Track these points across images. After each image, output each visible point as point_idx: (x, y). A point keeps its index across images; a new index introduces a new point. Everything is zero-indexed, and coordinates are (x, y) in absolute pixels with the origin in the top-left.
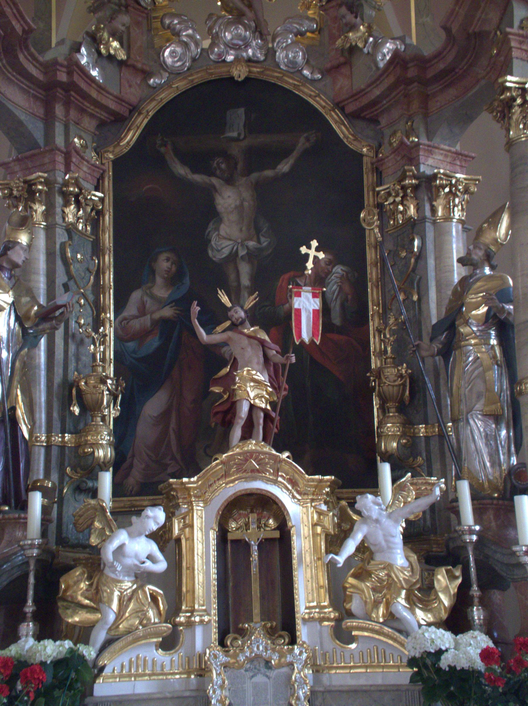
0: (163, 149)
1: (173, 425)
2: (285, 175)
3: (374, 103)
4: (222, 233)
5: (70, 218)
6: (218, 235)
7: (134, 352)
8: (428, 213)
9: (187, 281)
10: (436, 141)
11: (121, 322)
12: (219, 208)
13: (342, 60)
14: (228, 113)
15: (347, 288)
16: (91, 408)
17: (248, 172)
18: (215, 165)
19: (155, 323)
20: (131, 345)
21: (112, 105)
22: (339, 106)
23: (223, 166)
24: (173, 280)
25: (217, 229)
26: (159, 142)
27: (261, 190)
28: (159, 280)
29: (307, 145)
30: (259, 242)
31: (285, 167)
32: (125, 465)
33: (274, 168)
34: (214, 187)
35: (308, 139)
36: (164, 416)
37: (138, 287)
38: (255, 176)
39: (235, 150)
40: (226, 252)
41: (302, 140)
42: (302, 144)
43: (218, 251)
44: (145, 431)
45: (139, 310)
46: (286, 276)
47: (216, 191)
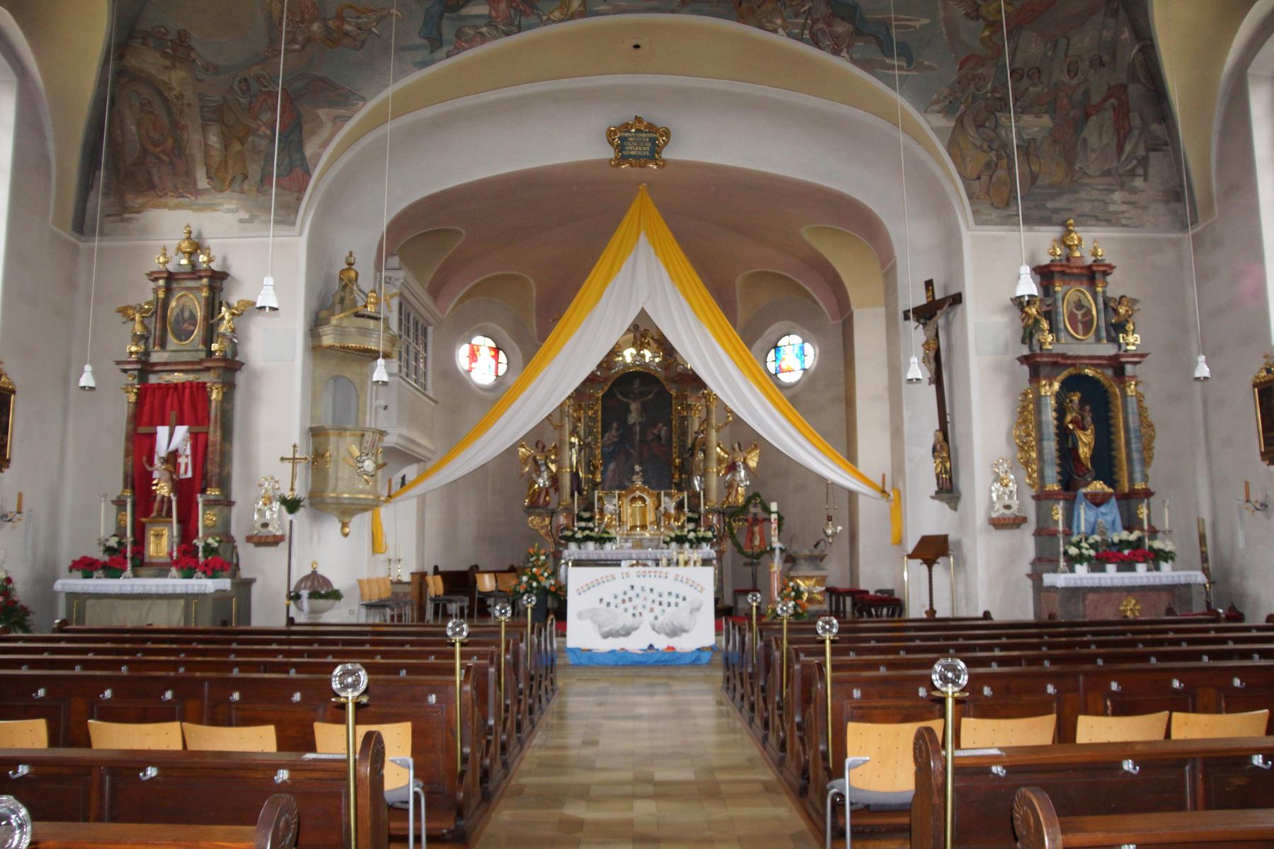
16: (596, 468)
36: (614, 471)
42: (656, 389)
44: (609, 473)
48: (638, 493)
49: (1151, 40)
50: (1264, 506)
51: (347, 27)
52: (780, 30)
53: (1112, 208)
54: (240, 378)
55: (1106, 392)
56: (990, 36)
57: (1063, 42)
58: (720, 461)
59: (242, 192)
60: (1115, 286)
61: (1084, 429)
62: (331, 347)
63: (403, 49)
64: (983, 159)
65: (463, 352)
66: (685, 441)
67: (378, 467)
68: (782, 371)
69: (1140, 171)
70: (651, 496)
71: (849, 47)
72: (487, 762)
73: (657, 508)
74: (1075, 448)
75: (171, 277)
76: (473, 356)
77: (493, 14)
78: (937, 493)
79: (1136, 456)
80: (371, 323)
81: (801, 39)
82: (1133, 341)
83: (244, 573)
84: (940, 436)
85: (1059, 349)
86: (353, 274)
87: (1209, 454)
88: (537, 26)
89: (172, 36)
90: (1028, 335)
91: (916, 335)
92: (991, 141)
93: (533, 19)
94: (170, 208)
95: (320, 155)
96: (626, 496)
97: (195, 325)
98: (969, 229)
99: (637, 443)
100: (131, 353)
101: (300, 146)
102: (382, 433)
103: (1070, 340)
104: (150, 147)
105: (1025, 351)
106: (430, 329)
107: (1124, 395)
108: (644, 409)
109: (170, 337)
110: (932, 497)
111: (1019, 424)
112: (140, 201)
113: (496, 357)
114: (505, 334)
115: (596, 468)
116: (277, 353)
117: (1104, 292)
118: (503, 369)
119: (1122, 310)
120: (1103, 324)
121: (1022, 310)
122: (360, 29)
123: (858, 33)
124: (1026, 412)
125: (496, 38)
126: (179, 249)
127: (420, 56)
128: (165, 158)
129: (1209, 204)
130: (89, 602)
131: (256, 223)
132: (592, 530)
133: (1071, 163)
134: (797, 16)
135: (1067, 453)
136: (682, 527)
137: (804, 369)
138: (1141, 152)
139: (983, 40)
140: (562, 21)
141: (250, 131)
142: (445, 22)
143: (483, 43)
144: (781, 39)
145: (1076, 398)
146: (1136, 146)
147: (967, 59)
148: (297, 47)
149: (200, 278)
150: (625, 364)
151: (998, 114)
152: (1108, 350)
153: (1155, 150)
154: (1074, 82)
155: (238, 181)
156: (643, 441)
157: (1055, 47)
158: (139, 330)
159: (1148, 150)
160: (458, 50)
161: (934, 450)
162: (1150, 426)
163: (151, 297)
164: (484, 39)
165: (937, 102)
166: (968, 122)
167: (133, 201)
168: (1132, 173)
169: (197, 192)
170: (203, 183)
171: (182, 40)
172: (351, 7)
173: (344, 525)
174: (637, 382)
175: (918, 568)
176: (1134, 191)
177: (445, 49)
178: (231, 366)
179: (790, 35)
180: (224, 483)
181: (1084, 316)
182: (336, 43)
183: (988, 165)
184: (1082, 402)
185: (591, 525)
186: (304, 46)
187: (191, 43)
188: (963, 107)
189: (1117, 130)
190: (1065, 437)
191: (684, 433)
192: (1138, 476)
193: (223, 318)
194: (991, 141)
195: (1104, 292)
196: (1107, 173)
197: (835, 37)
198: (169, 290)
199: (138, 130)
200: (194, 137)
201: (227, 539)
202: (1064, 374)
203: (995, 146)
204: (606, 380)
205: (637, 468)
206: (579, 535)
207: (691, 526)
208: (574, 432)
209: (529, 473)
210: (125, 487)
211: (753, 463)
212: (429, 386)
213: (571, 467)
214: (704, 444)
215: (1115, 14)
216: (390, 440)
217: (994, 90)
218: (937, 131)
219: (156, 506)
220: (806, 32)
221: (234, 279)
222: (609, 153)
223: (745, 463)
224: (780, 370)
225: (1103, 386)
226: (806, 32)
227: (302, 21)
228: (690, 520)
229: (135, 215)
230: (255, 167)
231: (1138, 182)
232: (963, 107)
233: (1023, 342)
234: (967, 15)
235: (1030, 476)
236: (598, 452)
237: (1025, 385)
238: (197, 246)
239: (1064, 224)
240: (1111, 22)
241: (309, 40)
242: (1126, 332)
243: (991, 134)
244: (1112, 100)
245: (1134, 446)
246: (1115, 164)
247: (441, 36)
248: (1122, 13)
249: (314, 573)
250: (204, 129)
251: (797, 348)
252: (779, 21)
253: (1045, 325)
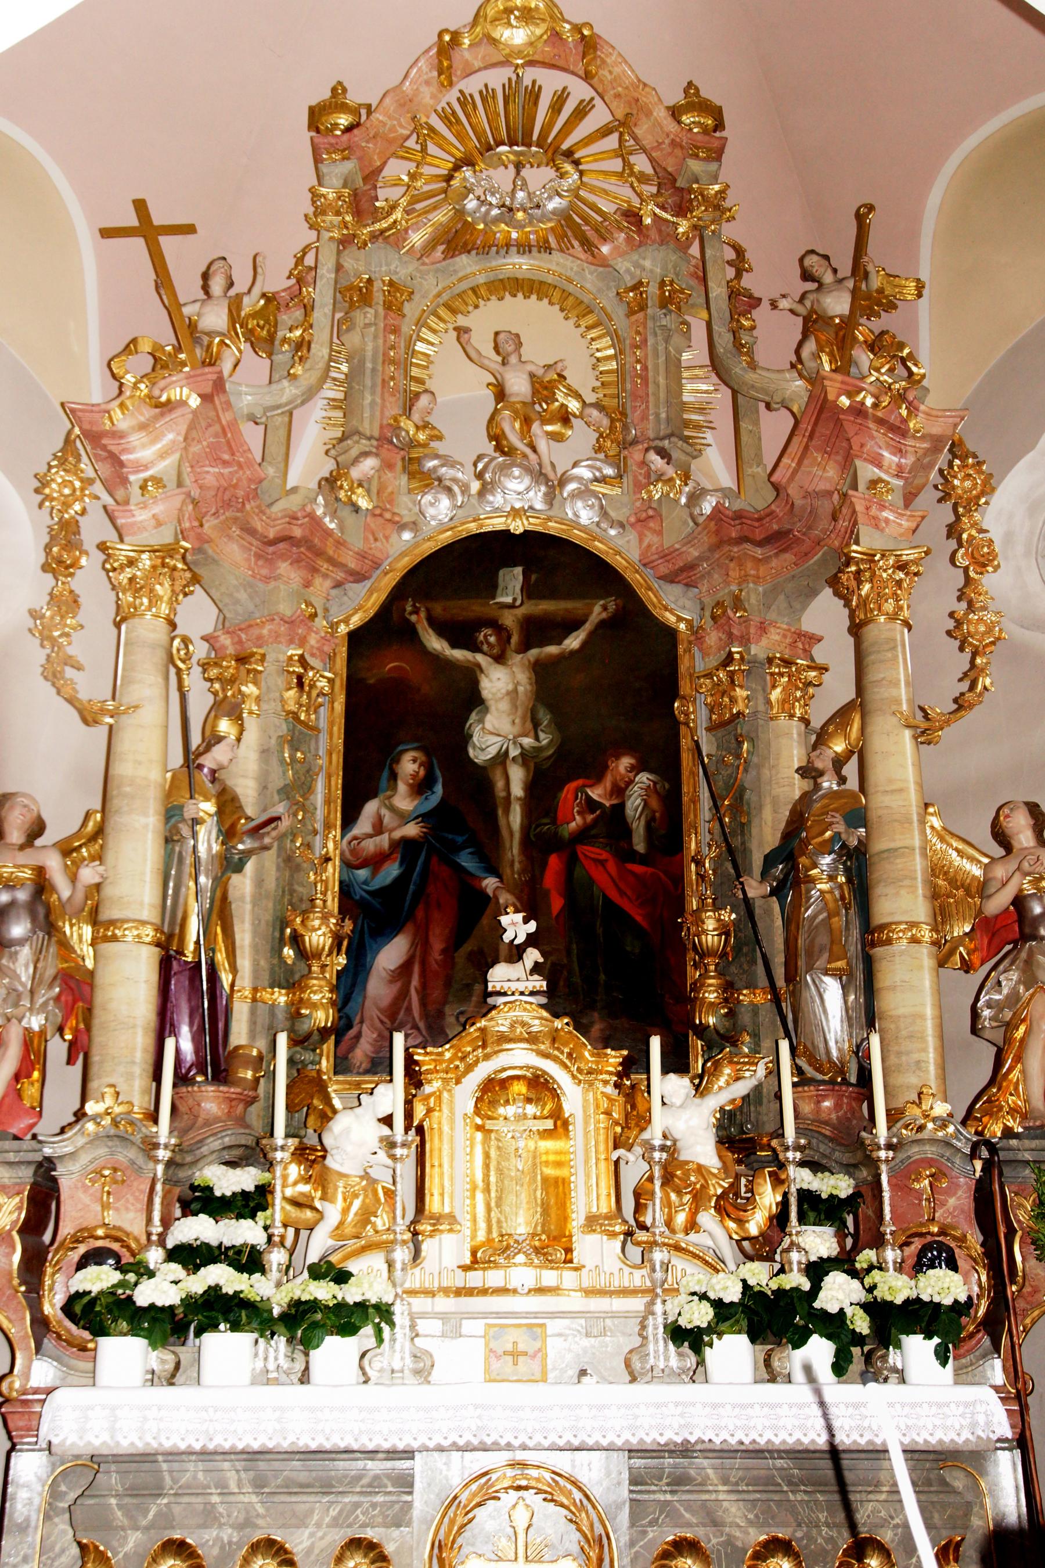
0: (413, 618)
1: (415, 982)
2: (573, 653)
3: (690, 567)
4: (488, 725)
5: (292, 707)
6: (483, 728)
7: (365, 883)
8: (761, 707)
9: (439, 789)
10: (772, 616)
11: (350, 843)
12: (486, 694)
13: (651, 513)
14: (501, 573)
15: (654, 803)
17: (525, 647)
18: (481, 638)
19: (395, 845)
20: (363, 873)
21: (352, 565)
23: (492, 639)
24: (421, 787)
25: (481, 721)
26: (409, 608)
27: (541, 670)
28: (402, 787)
29: (604, 615)
30: (537, 738)
31: (574, 642)
32: (352, 1033)
33: (560, 643)
34: (479, 666)
35: (605, 608)
36: (404, 970)
37: (375, 796)
38: (534, 653)
39: (509, 619)
40: (492, 751)
41: (597, 609)
42: (598, 612)
43: (483, 750)
44: (378, 988)
45: (374, 826)
46: (573, 785)
47: (482, 671)
48: (519, 1058)
70: (586, 1076)
99: (513, 850)
132: (249, 1261)
136: (763, 1248)
156: (539, 843)
174: (512, 582)
185: (245, 1232)
206: (164, 1288)
207: (818, 1241)
214: (858, 817)
228: (816, 1208)
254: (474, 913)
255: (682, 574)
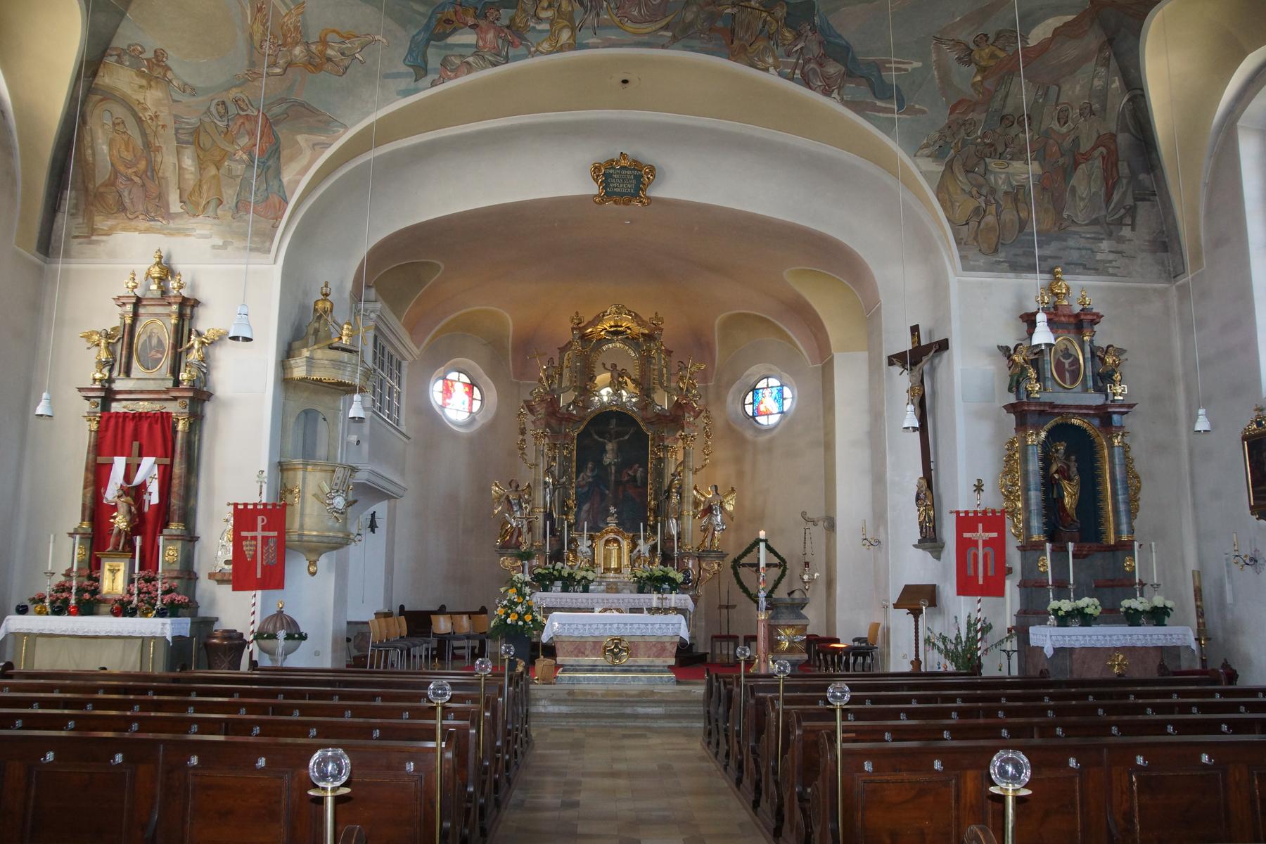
22: (643, 420)
24: (592, 470)
27: (619, 444)
36: (588, 511)
44: (583, 515)
48: (612, 536)
49: (1142, 90)
50: (1254, 560)
51: (330, 52)
52: (771, 69)
53: (1099, 257)
54: (209, 408)
55: (1092, 442)
56: (981, 82)
57: (1054, 89)
58: (696, 504)
59: (217, 217)
60: (1103, 336)
61: (1070, 479)
62: (303, 379)
63: (387, 76)
64: (972, 204)
65: (436, 389)
66: (661, 483)
67: (349, 504)
68: (761, 414)
69: (1128, 220)
71: (840, 88)
72: (467, 831)
73: (631, 551)
74: (1062, 498)
75: (138, 302)
76: (447, 391)
77: (481, 43)
78: (920, 541)
79: (1122, 507)
80: (345, 356)
81: (792, 79)
82: (1120, 391)
83: (202, 612)
84: (925, 484)
85: (1046, 398)
86: (328, 305)
87: (1195, 506)
88: (524, 57)
89: (149, 54)
90: (1015, 384)
91: (902, 380)
92: (979, 186)
93: (521, 50)
94: (140, 232)
95: (297, 182)
96: (600, 538)
97: (163, 353)
98: (956, 275)
100: (95, 380)
101: (278, 174)
102: (354, 470)
103: (1057, 388)
104: (122, 168)
105: (1012, 399)
106: (405, 364)
107: (1111, 446)
108: (620, 450)
109: (135, 364)
110: (915, 546)
111: (1005, 474)
112: (110, 223)
113: (470, 393)
114: (479, 371)
115: (570, 508)
116: (246, 384)
117: (1091, 341)
118: (476, 406)
119: (1109, 360)
120: (1089, 373)
121: (1009, 357)
122: (343, 54)
123: (850, 74)
124: (1011, 462)
125: (483, 68)
126: (148, 274)
127: (403, 84)
128: (136, 179)
129: (1197, 257)
130: (39, 640)
131: (230, 248)
133: (1059, 211)
134: (789, 56)
135: (1052, 505)
137: (782, 412)
138: (1129, 201)
139: (974, 85)
140: (550, 53)
141: (226, 155)
142: (431, 52)
143: (469, 73)
144: (772, 78)
145: (1061, 448)
146: (1124, 193)
147: (959, 103)
148: (278, 70)
149: (170, 304)
150: (602, 403)
151: (987, 160)
152: (1096, 399)
153: (1143, 200)
154: (1064, 130)
155: (213, 204)
156: (618, 483)
157: (1046, 94)
158: (104, 356)
159: (1136, 199)
160: (443, 79)
161: (918, 498)
162: (1137, 477)
163: (117, 322)
164: (470, 68)
165: (927, 146)
166: (957, 167)
167: (101, 222)
168: (1120, 223)
169: (168, 216)
170: (175, 206)
171: (159, 58)
172: (334, 31)
173: (313, 563)
174: (614, 422)
175: (902, 620)
176: (1121, 240)
177: (429, 78)
178: (200, 396)
179: (780, 74)
180: (188, 517)
181: (1071, 364)
182: (318, 68)
183: (977, 210)
184: (1068, 453)
186: (285, 70)
187: (169, 63)
188: (952, 151)
189: (1106, 179)
190: (1050, 486)
191: (660, 473)
192: (1124, 527)
193: (192, 346)
194: (979, 186)
195: (1091, 341)
196: (1095, 222)
197: (826, 78)
198: (136, 316)
199: (110, 150)
200: (167, 161)
201: (188, 574)
202: (1048, 426)
203: (984, 191)
204: (583, 419)
205: (612, 510)
208: (549, 471)
209: (501, 513)
210: (83, 520)
211: (729, 508)
212: (402, 422)
213: (545, 507)
215: (1106, 63)
216: (361, 477)
217: (984, 135)
218: (925, 174)
219: (112, 540)
220: (797, 72)
221: (203, 305)
222: (593, 189)
223: (722, 507)
224: (757, 412)
225: (1090, 436)
226: (797, 72)
227: (284, 45)
229: (104, 238)
230: (230, 192)
231: (1126, 232)
232: (952, 151)
233: (1010, 390)
234: (959, 59)
235: (1016, 527)
236: (572, 492)
237: (1012, 433)
238: (167, 271)
239: (1051, 271)
240: (1102, 70)
241: (290, 64)
242: (1113, 382)
243: (981, 180)
244: (1102, 149)
245: (1121, 498)
246: (1103, 213)
247: (426, 63)
248: (1113, 62)
249: (280, 612)
250: (178, 153)
251: (775, 391)
252: (770, 60)
253: (1032, 373)
254: (603, 497)
255: (649, 422)
